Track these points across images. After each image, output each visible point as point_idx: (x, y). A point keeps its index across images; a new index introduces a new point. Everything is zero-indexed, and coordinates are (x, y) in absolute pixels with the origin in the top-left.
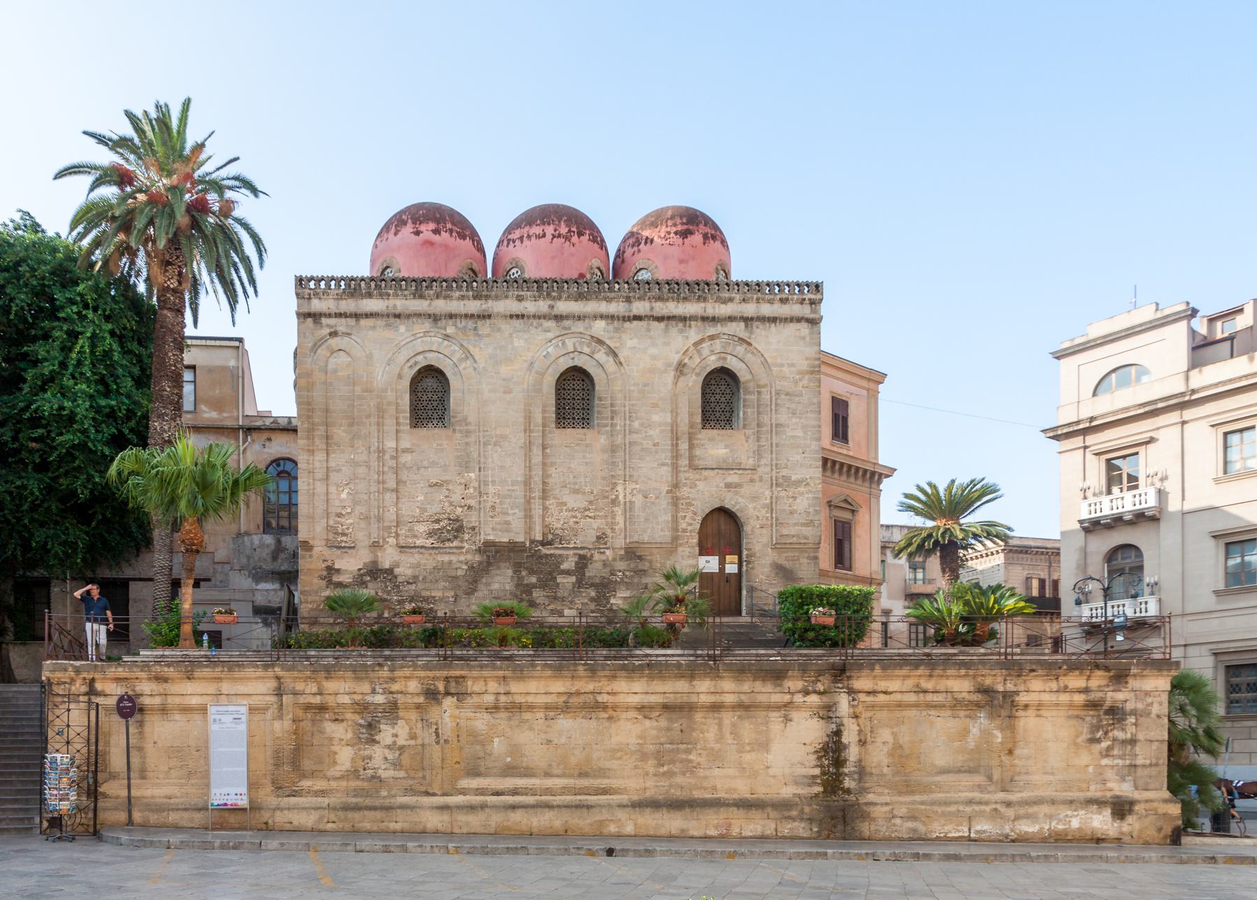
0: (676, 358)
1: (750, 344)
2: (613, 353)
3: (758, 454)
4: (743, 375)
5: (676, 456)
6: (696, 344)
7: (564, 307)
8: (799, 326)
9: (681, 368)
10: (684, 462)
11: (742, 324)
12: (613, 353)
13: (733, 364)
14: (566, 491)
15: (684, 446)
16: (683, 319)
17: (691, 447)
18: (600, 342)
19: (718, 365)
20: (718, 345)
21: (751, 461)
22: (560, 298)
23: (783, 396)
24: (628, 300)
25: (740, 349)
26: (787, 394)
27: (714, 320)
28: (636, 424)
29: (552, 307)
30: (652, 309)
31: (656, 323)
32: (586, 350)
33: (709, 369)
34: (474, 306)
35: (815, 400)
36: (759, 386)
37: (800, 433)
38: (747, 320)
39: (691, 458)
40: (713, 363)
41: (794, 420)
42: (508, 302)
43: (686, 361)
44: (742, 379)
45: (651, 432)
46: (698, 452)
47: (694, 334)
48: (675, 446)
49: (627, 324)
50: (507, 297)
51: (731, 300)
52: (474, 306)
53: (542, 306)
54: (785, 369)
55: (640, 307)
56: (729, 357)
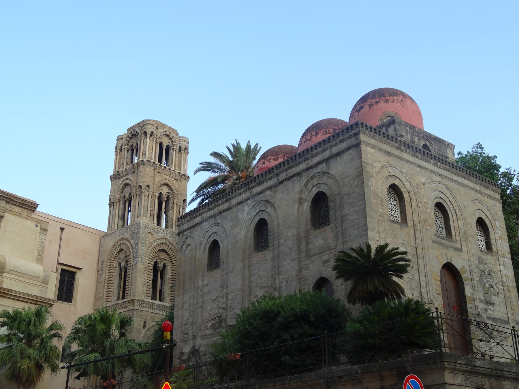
0: (297, 196)
1: (329, 173)
2: (273, 206)
3: (337, 238)
4: (328, 193)
5: (300, 253)
6: (306, 185)
7: (255, 190)
8: (350, 152)
9: (300, 201)
10: (304, 255)
11: (324, 164)
12: (273, 206)
13: (323, 189)
14: (258, 288)
15: (303, 245)
16: (299, 174)
17: (307, 244)
18: (268, 202)
19: (317, 191)
20: (315, 181)
21: (335, 243)
22: (253, 187)
23: (346, 197)
24: (277, 175)
25: (325, 179)
26: (348, 195)
27: (311, 167)
28: (282, 241)
29: (251, 193)
30: (287, 175)
31: (288, 182)
32: (264, 208)
33: (313, 196)
34: (226, 205)
35: (362, 193)
36: (335, 196)
37: (355, 217)
38: (327, 160)
39: (308, 251)
40: (315, 191)
41: (352, 209)
42: (237, 198)
43: (302, 196)
44: (328, 195)
45: (288, 243)
46: (310, 247)
47: (304, 179)
48: (299, 246)
49: (277, 188)
50: (236, 196)
51: (318, 154)
52: (226, 205)
53: (248, 194)
54: (346, 180)
55: (283, 176)
56: (321, 185)
